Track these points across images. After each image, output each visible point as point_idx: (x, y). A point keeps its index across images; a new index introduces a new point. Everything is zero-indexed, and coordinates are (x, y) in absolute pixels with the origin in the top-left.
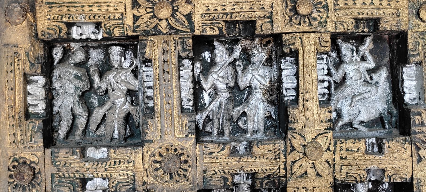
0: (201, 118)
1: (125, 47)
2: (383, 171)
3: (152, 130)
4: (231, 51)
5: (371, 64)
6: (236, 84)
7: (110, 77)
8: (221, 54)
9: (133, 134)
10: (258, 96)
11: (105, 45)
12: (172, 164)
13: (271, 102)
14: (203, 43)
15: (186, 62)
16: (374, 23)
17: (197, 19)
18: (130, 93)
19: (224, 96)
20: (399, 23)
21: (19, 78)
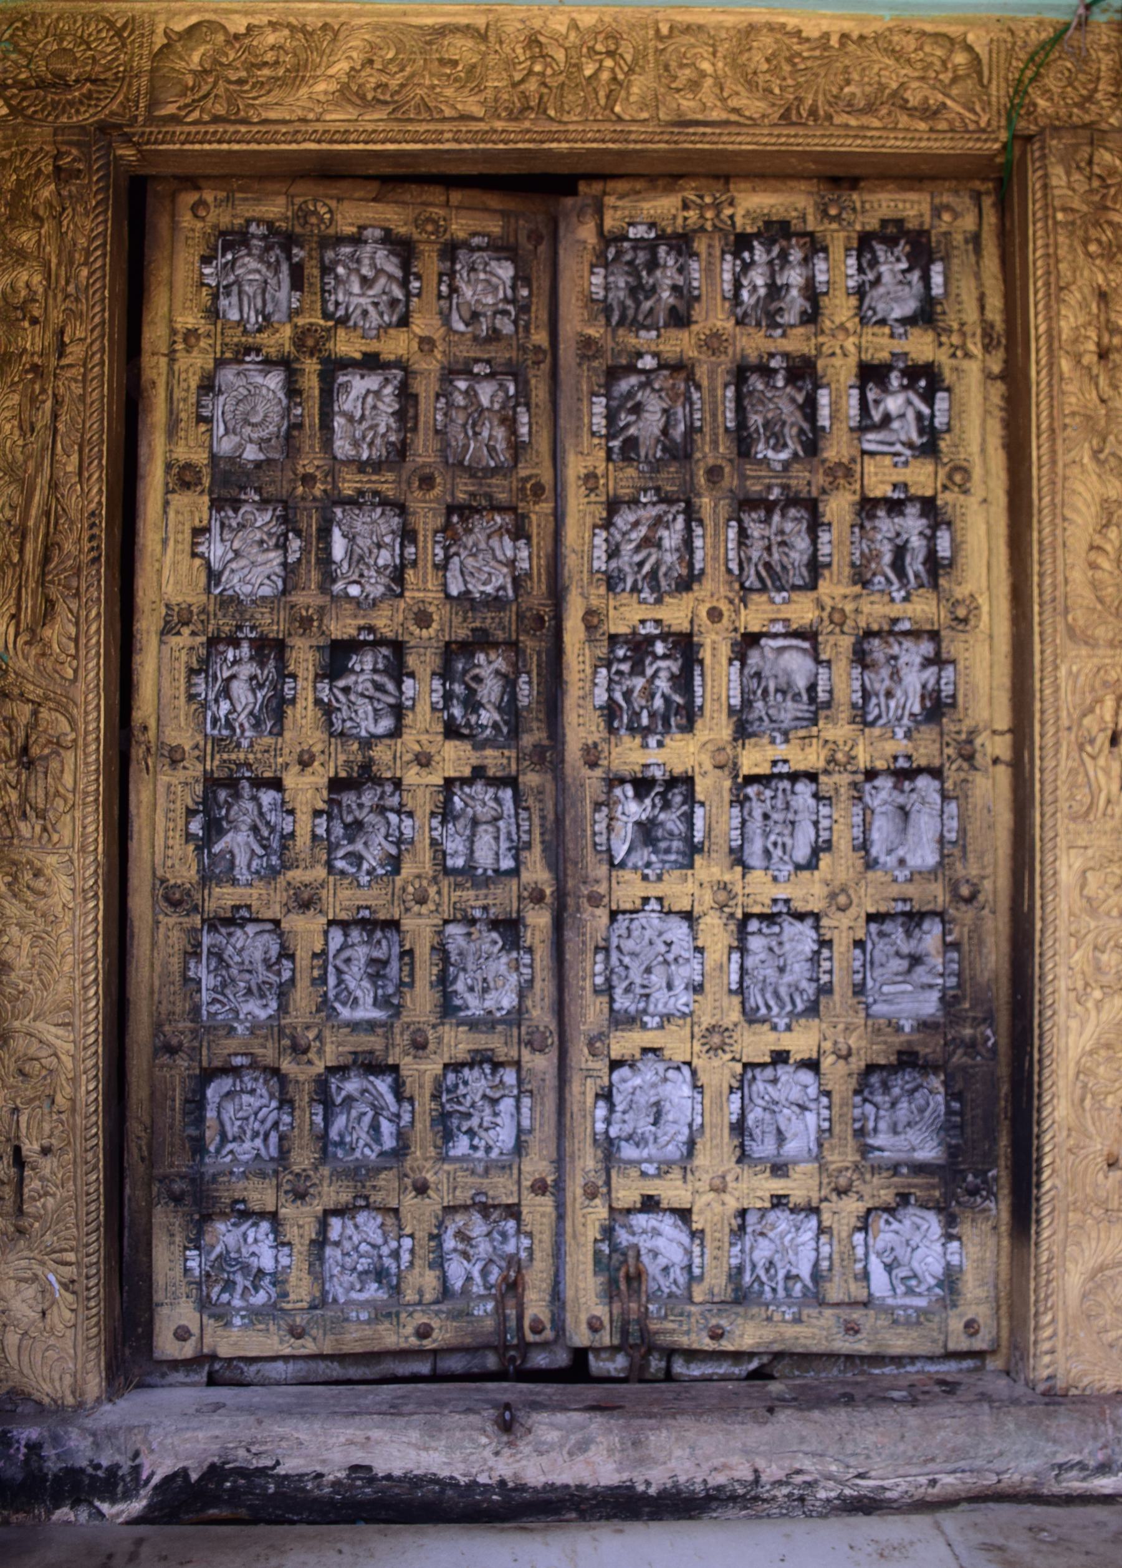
0: (739, 311)
1: (671, 248)
2: (906, 354)
3: (698, 312)
4: (769, 252)
5: (904, 265)
6: (774, 283)
7: (658, 273)
8: (760, 254)
9: (680, 319)
10: (794, 292)
11: (651, 247)
12: (714, 342)
13: (807, 299)
14: (742, 243)
15: (728, 257)
16: (899, 222)
17: (739, 221)
18: (675, 288)
19: (762, 292)
20: (922, 224)
21: (586, 268)
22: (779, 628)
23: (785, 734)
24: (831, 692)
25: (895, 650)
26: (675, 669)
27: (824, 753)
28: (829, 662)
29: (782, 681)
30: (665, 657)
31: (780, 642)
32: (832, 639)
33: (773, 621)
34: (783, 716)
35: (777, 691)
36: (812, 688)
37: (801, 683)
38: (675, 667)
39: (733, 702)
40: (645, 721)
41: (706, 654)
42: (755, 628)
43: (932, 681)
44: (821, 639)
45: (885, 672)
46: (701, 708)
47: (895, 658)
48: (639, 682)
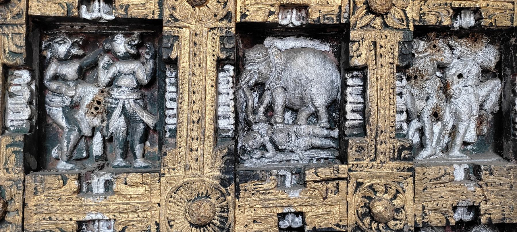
22: (291, 19)
23: (300, 173)
24: (364, 112)
25: (446, 56)
26: (143, 77)
27: (356, 200)
28: (363, 69)
29: (294, 95)
30: (128, 57)
31: (291, 43)
32: (370, 35)
33: (284, 7)
34: (293, 145)
35: (287, 108)
36: (336, 106)
37: (320, 100)
38: (142, 71)
39: (222, 124)
40: (97, 149)
41: (183, 51)
42: (257, 16)
43: (494, 98)
44: (353, 35)
45: (432, 86)
46: (174, 133)
47: (442, 67)
48: (89, 93)
